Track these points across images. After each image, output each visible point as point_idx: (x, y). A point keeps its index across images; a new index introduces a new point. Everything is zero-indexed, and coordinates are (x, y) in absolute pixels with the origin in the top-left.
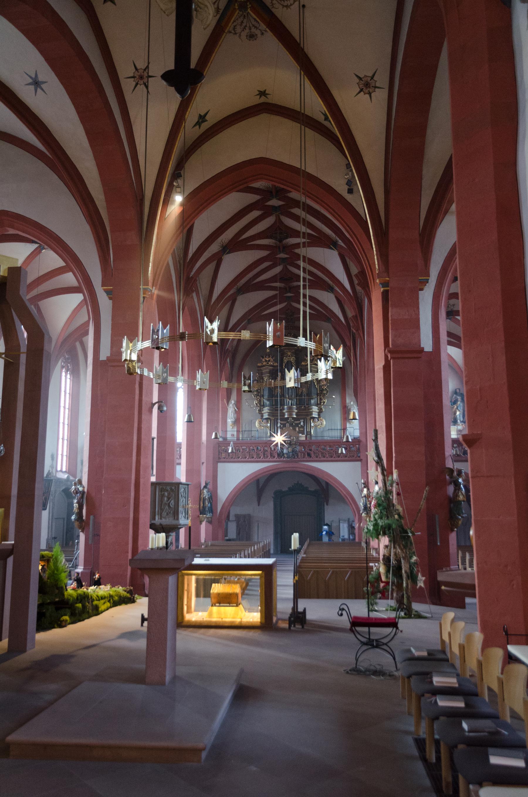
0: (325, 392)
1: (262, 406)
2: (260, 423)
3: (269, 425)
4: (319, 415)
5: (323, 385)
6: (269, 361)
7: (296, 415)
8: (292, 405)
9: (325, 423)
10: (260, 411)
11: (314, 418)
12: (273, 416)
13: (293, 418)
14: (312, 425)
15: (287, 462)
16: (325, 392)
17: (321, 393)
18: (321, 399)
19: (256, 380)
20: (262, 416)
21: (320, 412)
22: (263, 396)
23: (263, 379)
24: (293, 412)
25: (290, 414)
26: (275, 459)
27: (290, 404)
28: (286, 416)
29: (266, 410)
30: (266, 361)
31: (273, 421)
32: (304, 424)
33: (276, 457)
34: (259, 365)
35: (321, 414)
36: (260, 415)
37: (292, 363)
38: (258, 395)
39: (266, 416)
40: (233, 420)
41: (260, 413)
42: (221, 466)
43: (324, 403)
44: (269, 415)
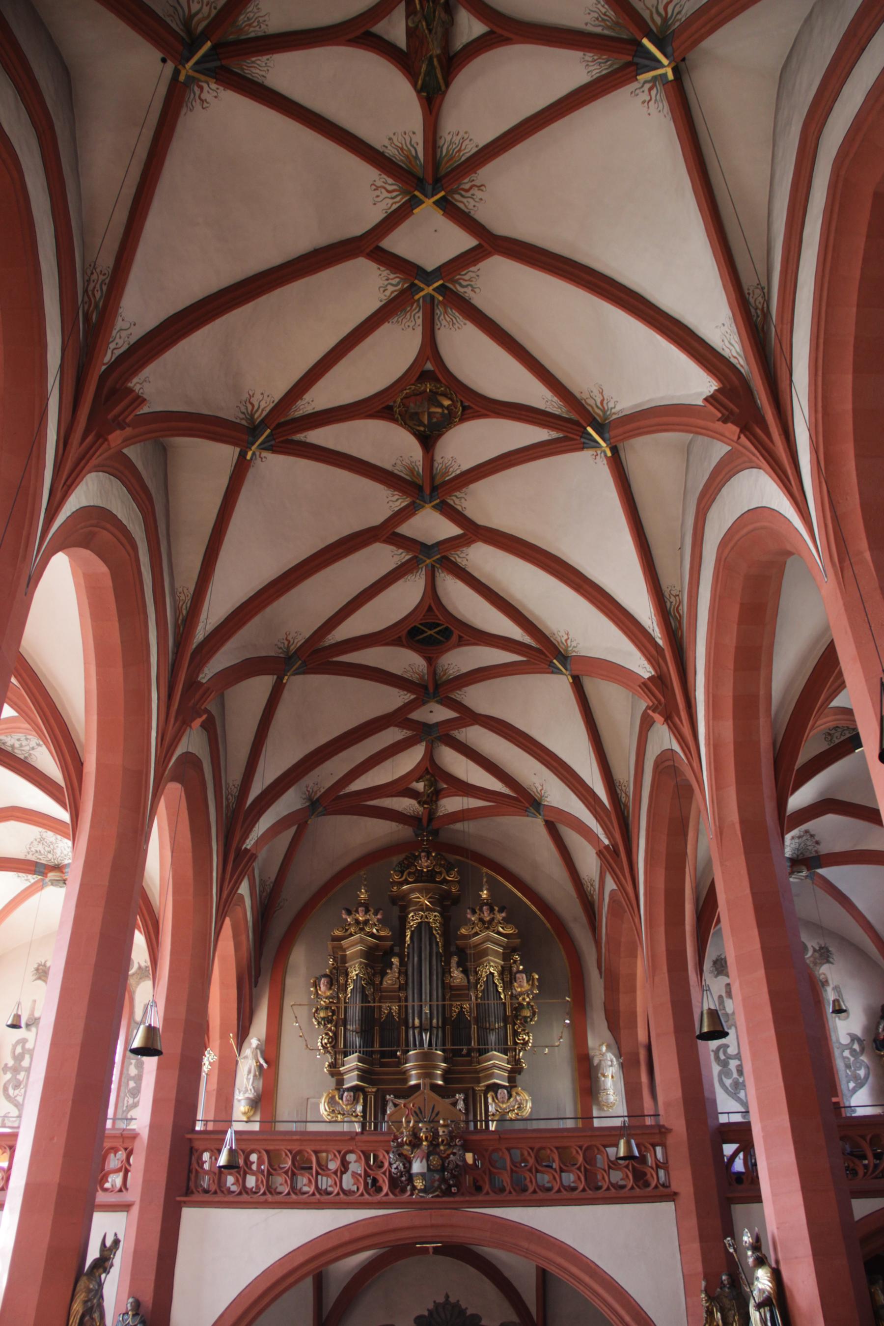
0: (527, 1013)
1: (337, 1049)
2: (331, 1101)
3: (359, 1108)
4: (512, 1080)
5: (521, 994)
6: (366, 922)
7: (444, 1078)
8: (430, 1044)
9: (529, 1104)
10: (333, 1065)
11: (495, 1088)
12: (372, 1083)
13: (434, 1088)
14: (492, 1109)
15: (420, 1205)
16: (527, 1013)
17: (516, 1017)
18: (516, 1034)
19: (325, 976)
20: (340, 1082)
21: (515, 1071)
22: (345, 1022)
23: (347, 974)
24: (436, 1067)
25: (427, 1074)
26: (380, 1197)
27: (426, 1045)
28: (413, 1082)
29: (352, 1062)
30: (357, 922)
31: (371, 1098)
32: (467, 1109)
33: (385, 1189)
34: (337, 933)
35: (519, 1078)
36: (332, 1082)
37: (431, 928)
38: (330, 1022)
39: (351, 1080)
40: (251, 1094)
41: (332, 1074)
42: (190, 1216)
43: (526, 1043)
44: (360, 1078)
